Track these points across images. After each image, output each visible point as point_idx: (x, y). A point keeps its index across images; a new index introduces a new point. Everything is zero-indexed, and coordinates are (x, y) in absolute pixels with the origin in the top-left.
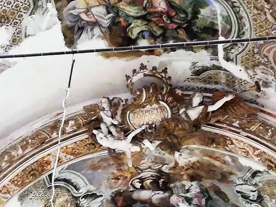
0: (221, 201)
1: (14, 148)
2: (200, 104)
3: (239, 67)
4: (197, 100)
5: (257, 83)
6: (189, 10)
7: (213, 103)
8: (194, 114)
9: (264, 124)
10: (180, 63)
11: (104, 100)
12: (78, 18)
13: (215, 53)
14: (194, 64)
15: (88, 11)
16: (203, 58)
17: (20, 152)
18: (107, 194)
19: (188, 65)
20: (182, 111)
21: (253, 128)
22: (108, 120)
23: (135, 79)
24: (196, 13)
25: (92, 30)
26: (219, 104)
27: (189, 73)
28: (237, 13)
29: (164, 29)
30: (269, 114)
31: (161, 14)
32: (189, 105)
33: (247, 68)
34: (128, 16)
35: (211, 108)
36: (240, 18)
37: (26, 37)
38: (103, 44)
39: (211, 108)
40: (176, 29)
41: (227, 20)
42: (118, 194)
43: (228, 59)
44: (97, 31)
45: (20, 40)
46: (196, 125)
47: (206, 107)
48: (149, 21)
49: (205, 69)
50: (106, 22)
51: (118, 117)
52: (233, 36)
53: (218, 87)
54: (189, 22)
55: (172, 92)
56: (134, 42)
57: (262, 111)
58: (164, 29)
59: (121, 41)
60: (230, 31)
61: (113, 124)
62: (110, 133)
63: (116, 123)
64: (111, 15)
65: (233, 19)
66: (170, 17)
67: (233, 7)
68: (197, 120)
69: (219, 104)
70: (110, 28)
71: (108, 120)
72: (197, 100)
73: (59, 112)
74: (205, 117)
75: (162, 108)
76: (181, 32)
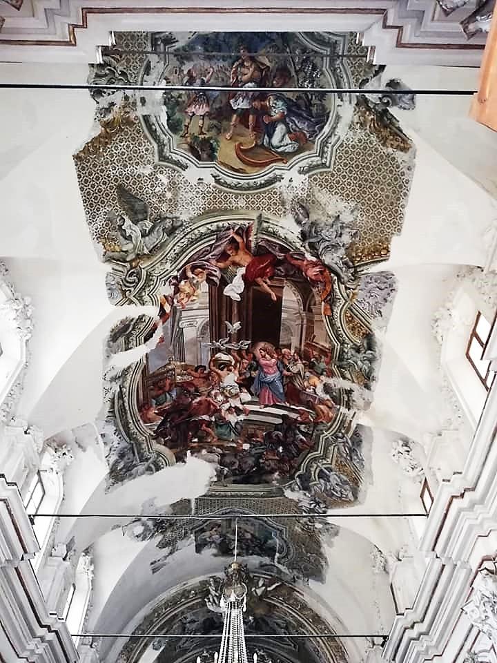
0: (264, 625)
1: (160, 608)
2: (263, 585)
3: (285, 567)
4: (261, 583)
5: (294, 578)
6: (263, 540)
7: (270, 587)
8: (259, 592)
9: (296, 600)
10: (254, 560)
11: (211, 579)
12: (205, 540)
13: (273, 559)
14: (261, 562)
15: (210, 537)
16: (266, 560)
17: (164, 610)
18: (202, 620)
19: (258, 562)
20: (253, 589)
21: (291, 602)
22: (213, 593)
23: (230, 570)
24: (266, 542)
25: (211, 544)
26: (274, 586)
27: (257, 566)
28: (287, 546)
29: (248, 546)
30: (300, 593)
31: (248, 539)
32: (257, 586)
33: (288, 569)
34: (230, 539)
35: (269, 589)
36: (288, 548)
37: (177, 550)
38: (215, 551)
39: (269, 589)
40: (254, 547)
41: (282, 547)
42: (208, 619)
43: (279, 563)
44: (213, 545)
45: (174, 552)
46: (260, 598)
47: (266, 588)
48: (241, 542)
49: (266, 565)
50: (218, 541)
51: (219, 592)
52: (284, 554)
53: (272, 574)
54: (262, 545)
55: (248, 577)
56: (231, 550)
57: (295, 590)
58: (248, 546)
59: (225, 550)
60: (283, 551)
61: (215, 595)
62: (214, 600)
63: (217, 595)
64: (222, 539)
65: (285, 548)
66: (252, 542)
67: (285, 541)
68: (261, 596)
69: (274, 586)
70: (220, 544)
71: (213, 593)
72: (261, 583)
73: (185, 582)
74: (265, 593)
75: (243, 587)
76: (257, 548)
